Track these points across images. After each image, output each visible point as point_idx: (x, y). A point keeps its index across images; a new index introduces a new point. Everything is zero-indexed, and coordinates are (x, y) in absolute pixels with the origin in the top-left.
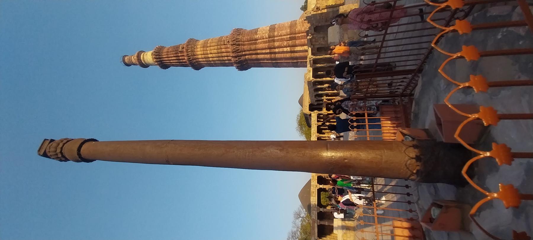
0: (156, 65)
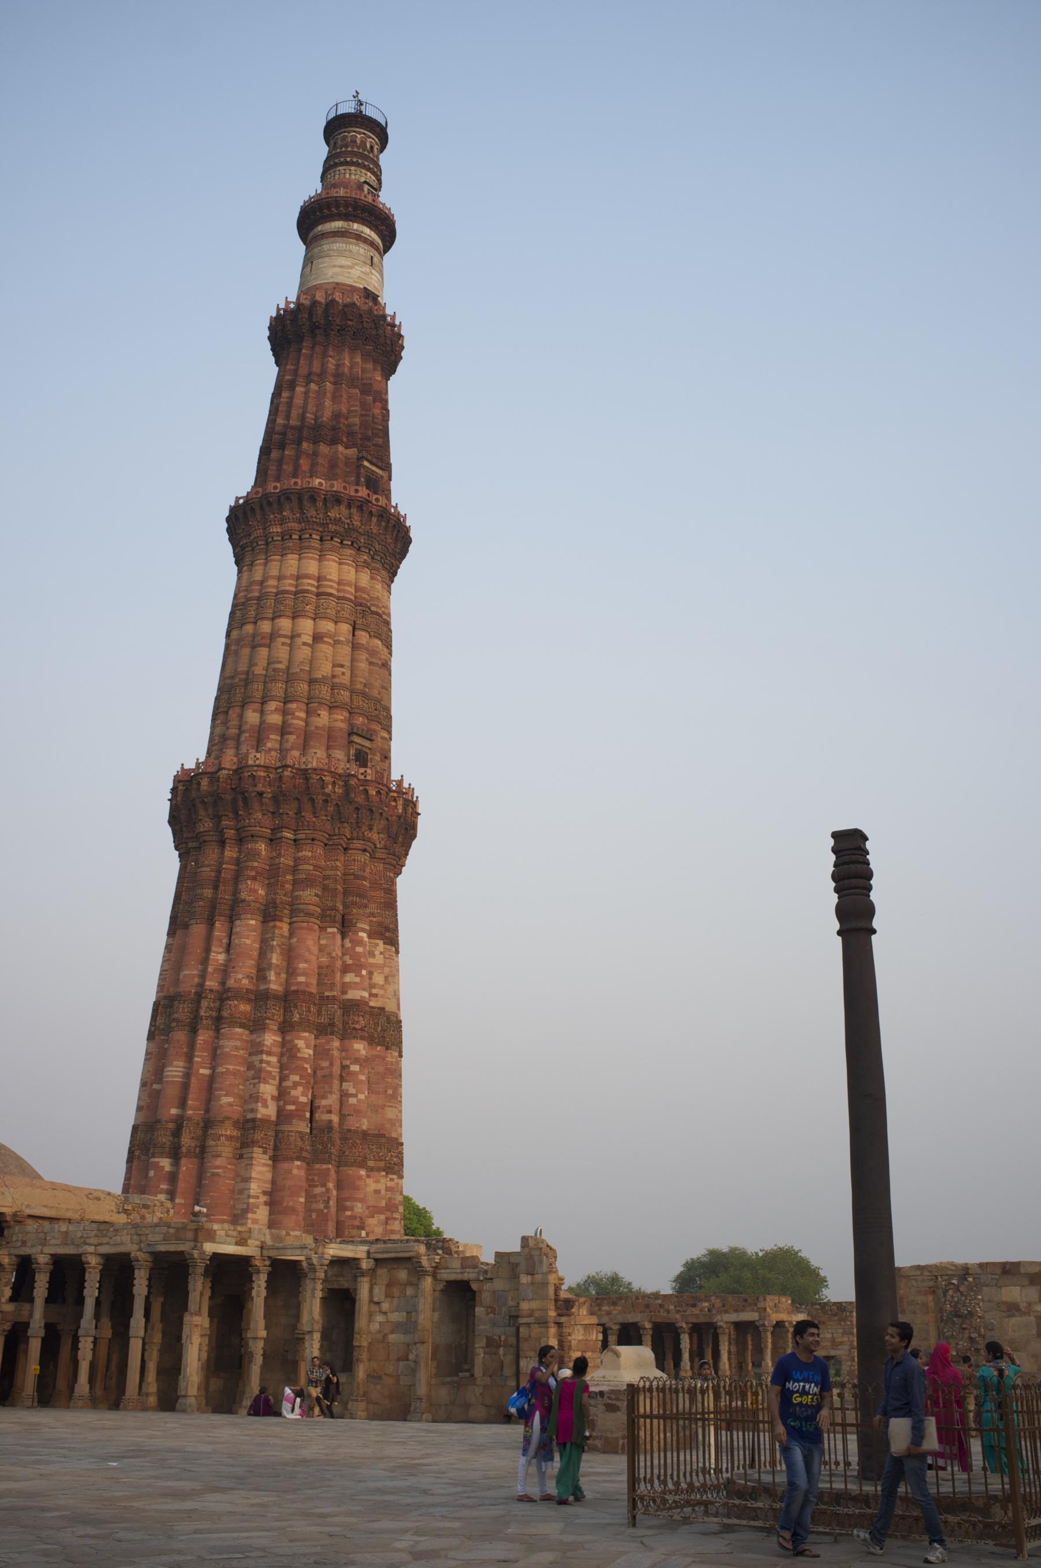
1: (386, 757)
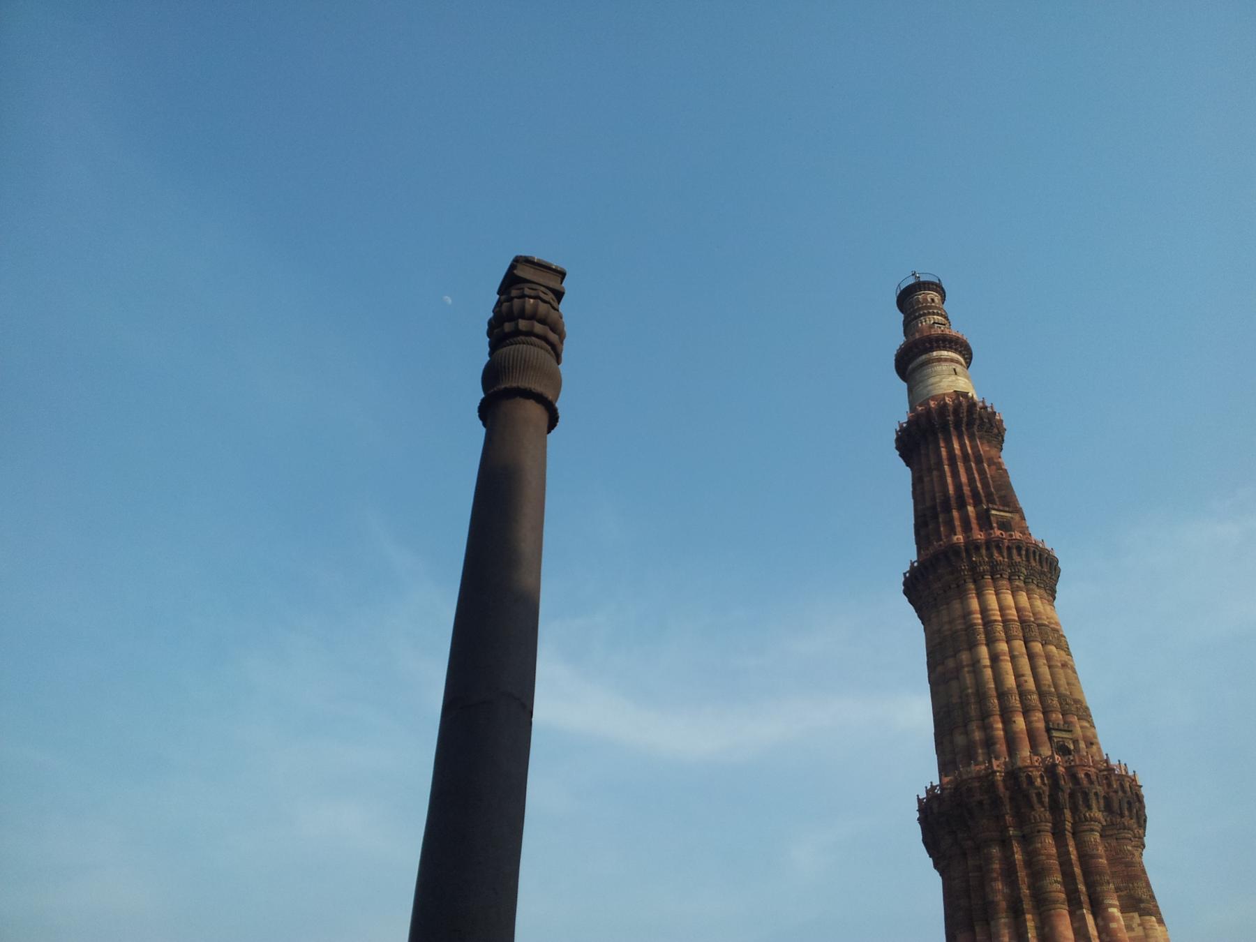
0: (912, 409)
1: (1091, 743)
